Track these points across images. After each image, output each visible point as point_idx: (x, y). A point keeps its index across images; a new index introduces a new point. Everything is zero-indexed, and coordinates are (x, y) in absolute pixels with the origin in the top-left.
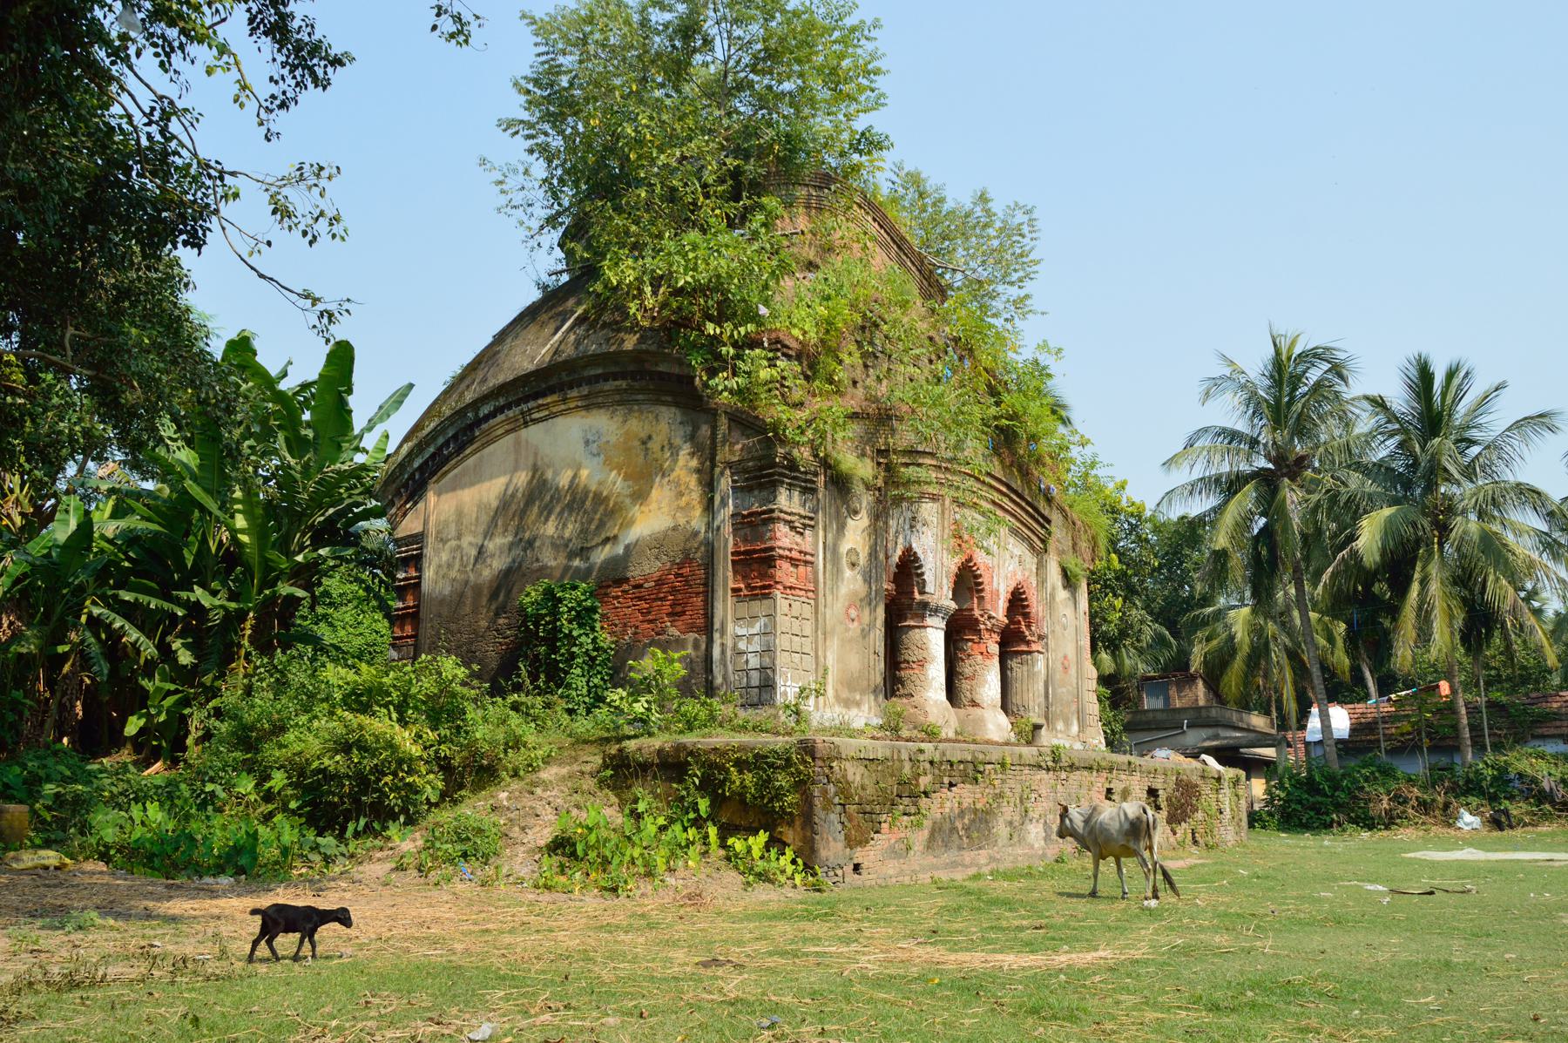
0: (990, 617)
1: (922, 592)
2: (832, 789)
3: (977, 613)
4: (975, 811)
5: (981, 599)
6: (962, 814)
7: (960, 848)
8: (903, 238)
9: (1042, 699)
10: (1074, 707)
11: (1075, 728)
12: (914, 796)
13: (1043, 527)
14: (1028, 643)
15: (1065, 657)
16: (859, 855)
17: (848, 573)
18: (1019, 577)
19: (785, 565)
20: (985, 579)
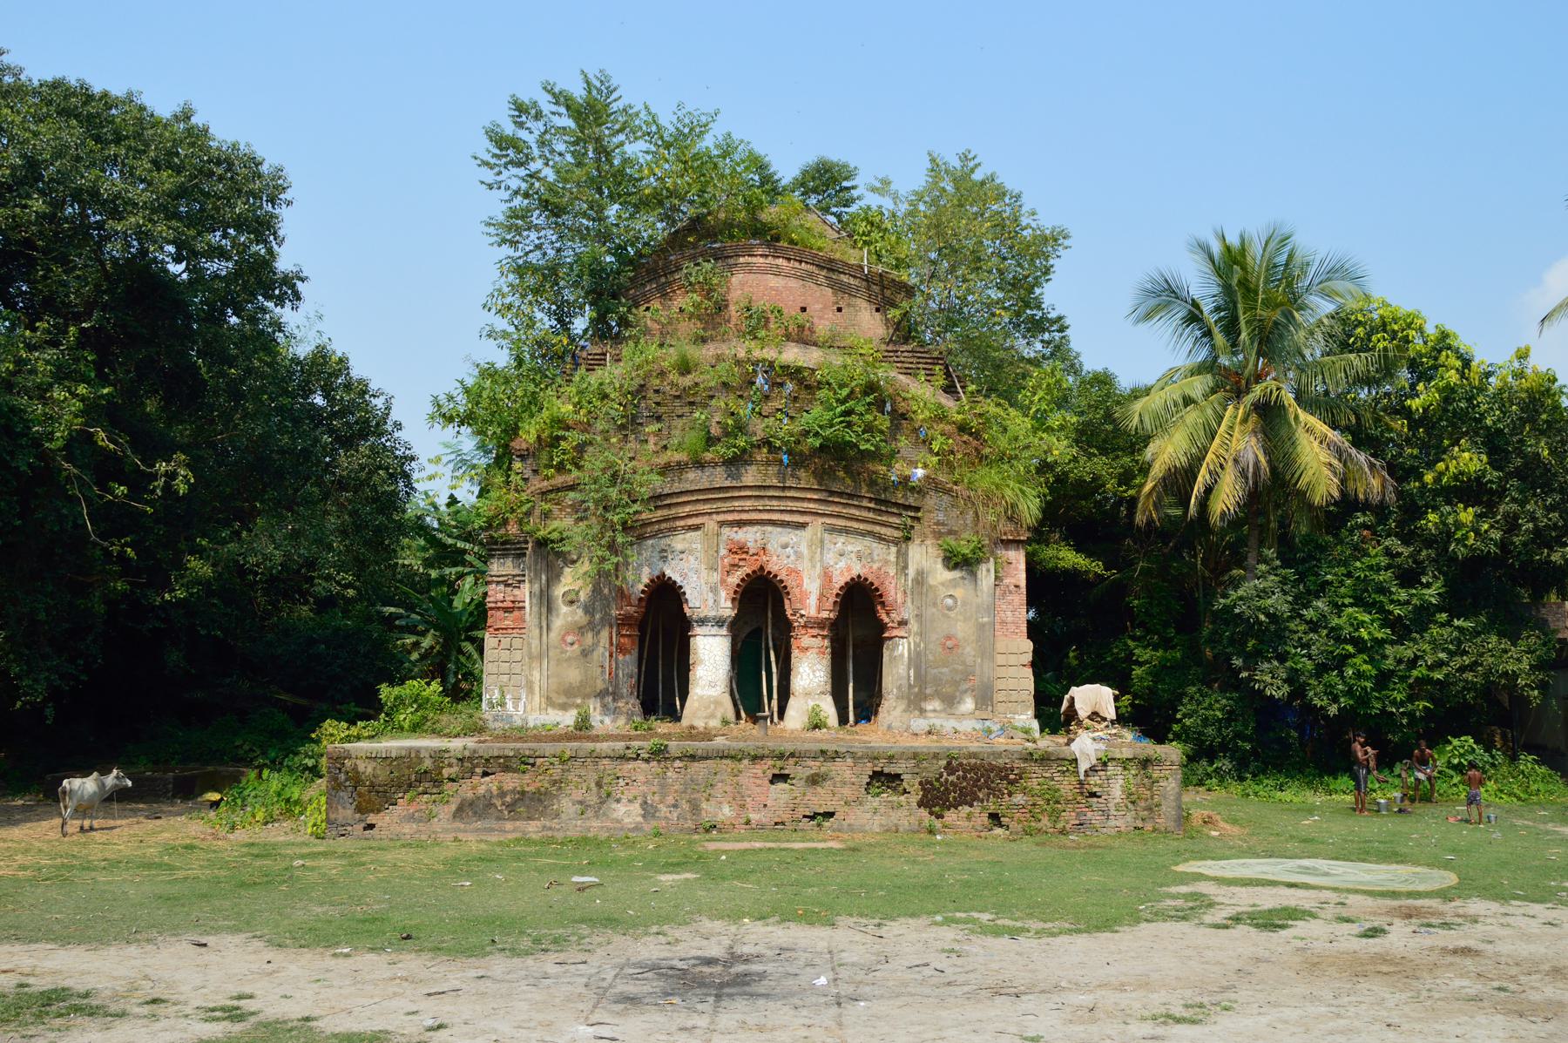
2: (342, 777)
4: (523, 793)
6: (502, 794)
7: (498, 819)
8: (831, 261)
9: (904, 682)
11: (968, 704)
12: (437, 782)
16: (372, 818)
17: (564, 609)
18: (857, 569)
19: (500, 614)
20: (790, 582)
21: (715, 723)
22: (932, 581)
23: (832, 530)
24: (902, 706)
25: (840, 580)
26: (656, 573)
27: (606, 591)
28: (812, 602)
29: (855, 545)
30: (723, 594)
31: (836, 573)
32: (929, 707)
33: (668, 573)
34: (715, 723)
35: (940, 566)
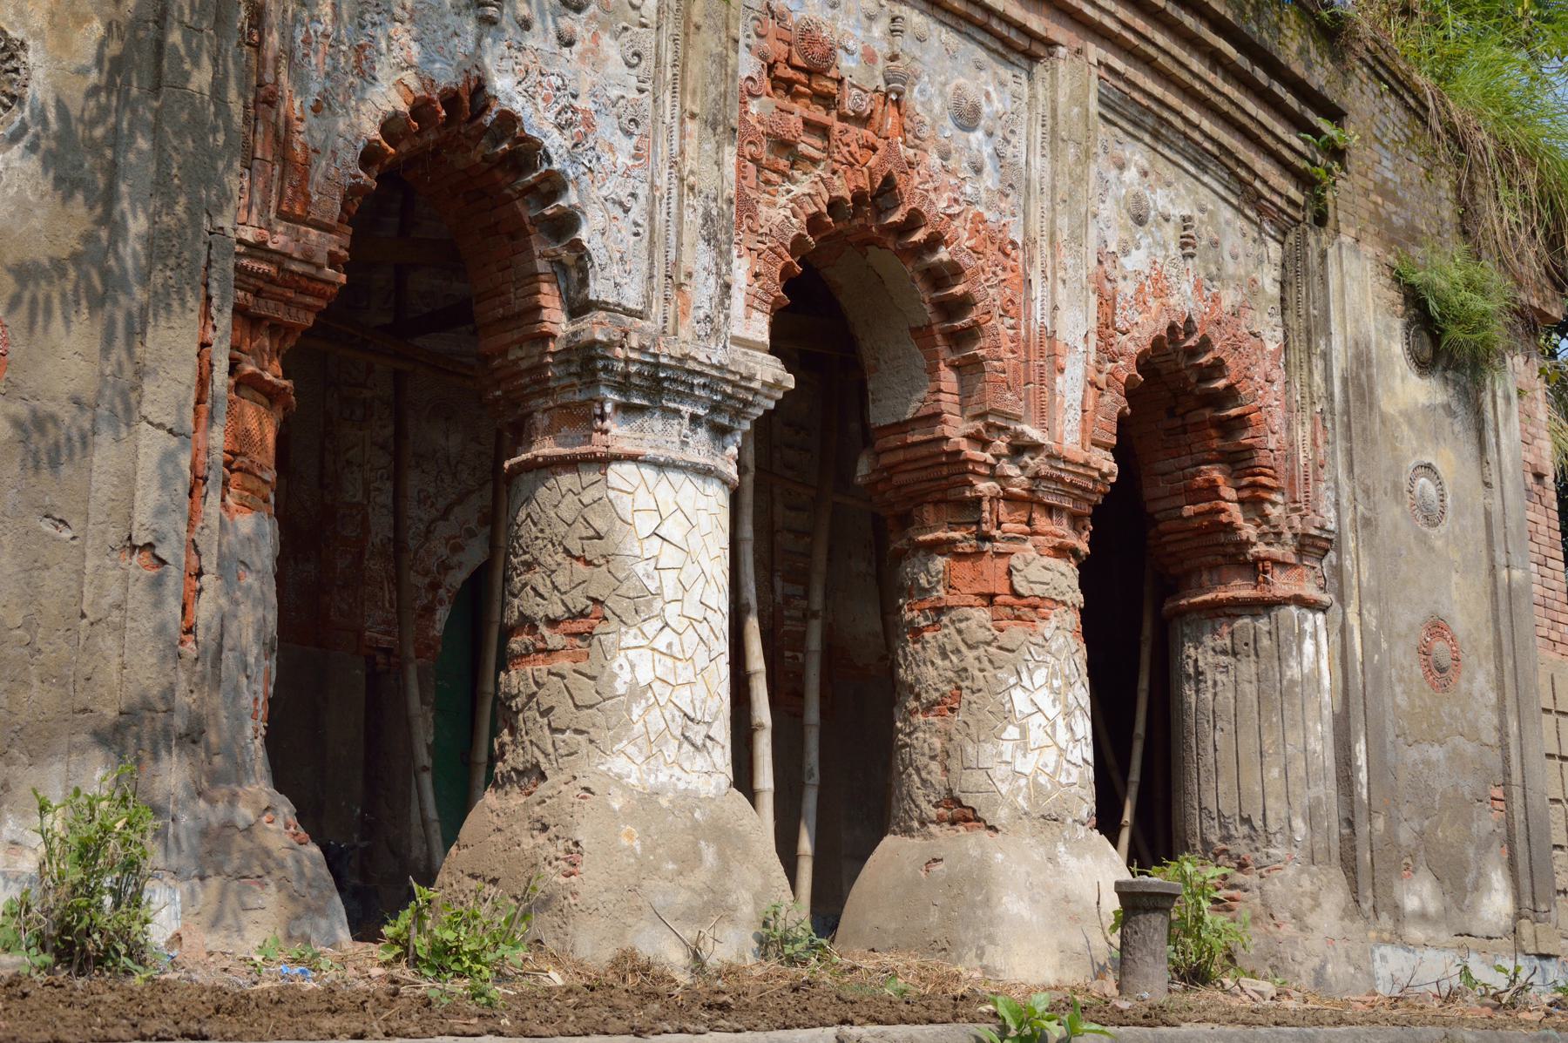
0: (1020, 448)
1: (578, 308)
3: (956, 429)
5: (970, 369)
9: (1327, 790)
10: (1488, 821)
11: (1497, 903)
13: (1299, 124)
14: (1256, 569)
15: (1438, 627)
18: (1184, 299)
20: (985, 287)
21: (731, 946)
22: (1386, 405)
23: (1125, 111)
24: (1336, 896)
25: (1142, 328)
26: (447, 76)
27: (201, 79)
28: (1070, 386)
29: (1181, 195)
30: (741, 271)
31: (1127, 289)
32: (1411, 903)
33: (502, 84)
34: (731, 946)
35: (1398, 348)
